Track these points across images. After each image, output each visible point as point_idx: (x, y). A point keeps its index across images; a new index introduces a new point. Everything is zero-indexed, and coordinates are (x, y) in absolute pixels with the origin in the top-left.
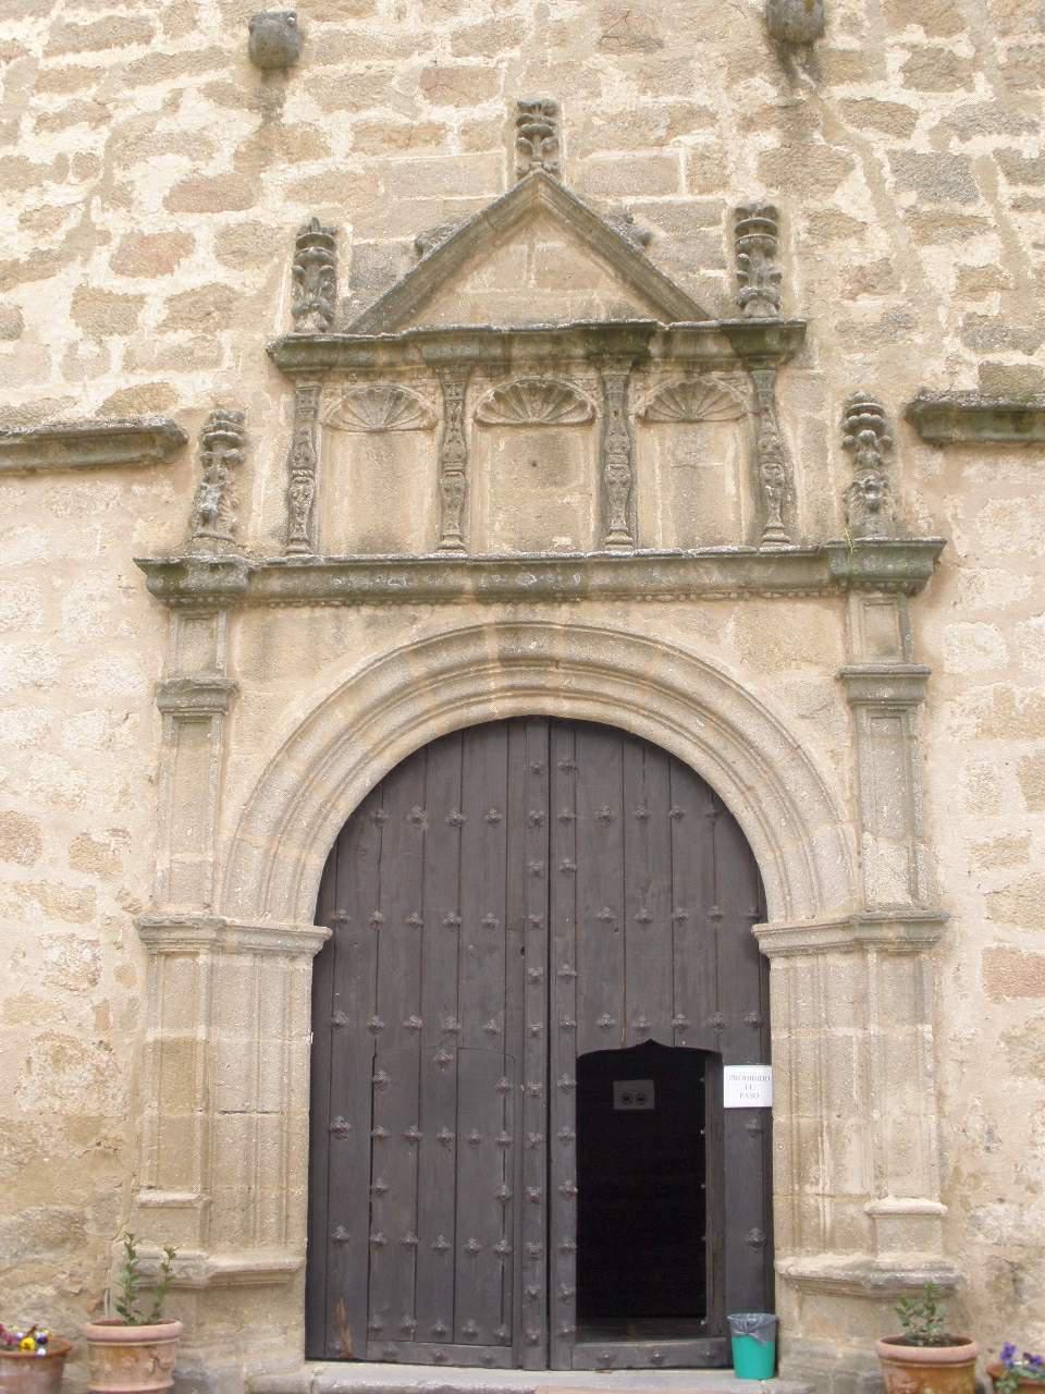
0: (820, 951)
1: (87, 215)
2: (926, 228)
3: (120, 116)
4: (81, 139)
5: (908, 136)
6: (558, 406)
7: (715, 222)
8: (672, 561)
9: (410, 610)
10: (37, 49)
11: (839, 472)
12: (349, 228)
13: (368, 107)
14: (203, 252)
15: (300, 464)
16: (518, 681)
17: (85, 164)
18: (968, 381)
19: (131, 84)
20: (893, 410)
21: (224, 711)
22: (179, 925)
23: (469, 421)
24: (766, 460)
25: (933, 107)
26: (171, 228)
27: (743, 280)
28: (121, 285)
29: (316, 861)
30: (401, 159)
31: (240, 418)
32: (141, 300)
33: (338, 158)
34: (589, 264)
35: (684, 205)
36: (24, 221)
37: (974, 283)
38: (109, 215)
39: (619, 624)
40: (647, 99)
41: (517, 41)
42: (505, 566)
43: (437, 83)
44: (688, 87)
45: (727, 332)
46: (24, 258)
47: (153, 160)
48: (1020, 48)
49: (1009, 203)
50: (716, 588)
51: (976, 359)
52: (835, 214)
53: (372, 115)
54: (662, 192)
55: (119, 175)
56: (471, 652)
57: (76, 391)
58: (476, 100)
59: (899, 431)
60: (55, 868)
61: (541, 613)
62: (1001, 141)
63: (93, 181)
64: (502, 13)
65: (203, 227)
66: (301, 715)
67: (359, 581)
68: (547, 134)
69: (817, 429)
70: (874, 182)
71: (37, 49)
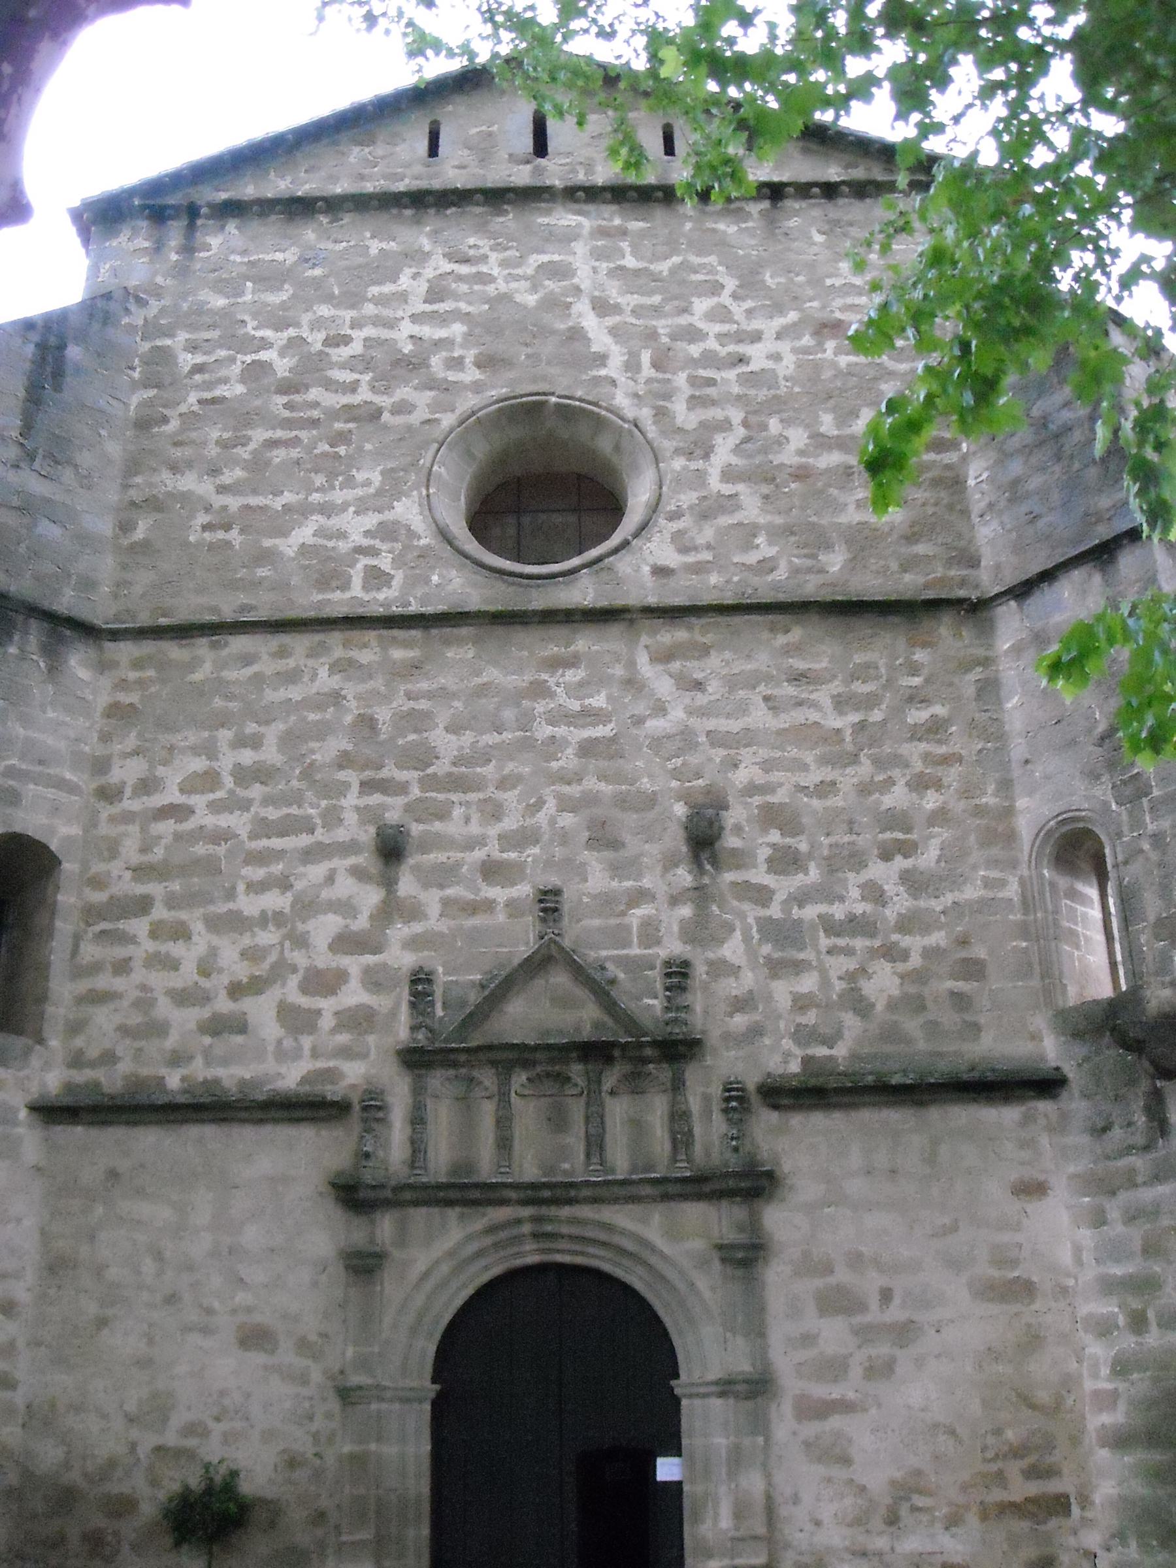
0: (705, 1396)
1: (282, 952)
2: (776, 968)
3: (299, 885)
4: (275, 901)
5: (768, 907)
6: (563, 1084)
7: (652, 968)
8: (624, 1183)
9: (481, 1209)
10: (244, 834)
11: (719, 1125)
12: (440, 970)
13: (449, 886)
14: (354, 983)
15: (417, 1119)
16: (542, 1246)
17: (278, 918)
18: (795, 1067)
20: (751, 1087)
21: (379, 1266)
22: (360, 1388)
23: (513, 1094)
24: (679, 1118)
25: (784, 886)
26: (334, 965)
27: (667, 1009)
28: (304, 1001)
29: (432, 1349)
31: (382, 1092)
32: (319, 1012)
33: (432, 922)
34: (581, 993)
35: (636, 956)
36: (244, 954)
37: (801, 1003)
38: (295, 954)
39: (597, 1217)
40: (615, 884)
41: (537, 841)
42: (533, 1186)
43: (492, 871)
44: (639, 876)
45: (655, 1044)
46: (245, 980)
47: (321, 918)
48: (837, 845)
49: (824, 950)
50: (647, 1196)
51: (799, 1052)
52: (724, 962)
53: (450, 892)
54: (624, 948)
55: (300, 927)
56: (515, 1231)
57: (283, 1070)
58: (513, 884)
59: (755, 1099)
60: (287, 1355)
61: (553, 1211)
62: (822, 908)
63: (284, 931)
64: (529, 822)
65: (354, 964)
66: (423, 1269)
67: (453, 1194)
68: (556, 910)
69: (707, 1098)
70: (747, 939)
71: (244, 834)
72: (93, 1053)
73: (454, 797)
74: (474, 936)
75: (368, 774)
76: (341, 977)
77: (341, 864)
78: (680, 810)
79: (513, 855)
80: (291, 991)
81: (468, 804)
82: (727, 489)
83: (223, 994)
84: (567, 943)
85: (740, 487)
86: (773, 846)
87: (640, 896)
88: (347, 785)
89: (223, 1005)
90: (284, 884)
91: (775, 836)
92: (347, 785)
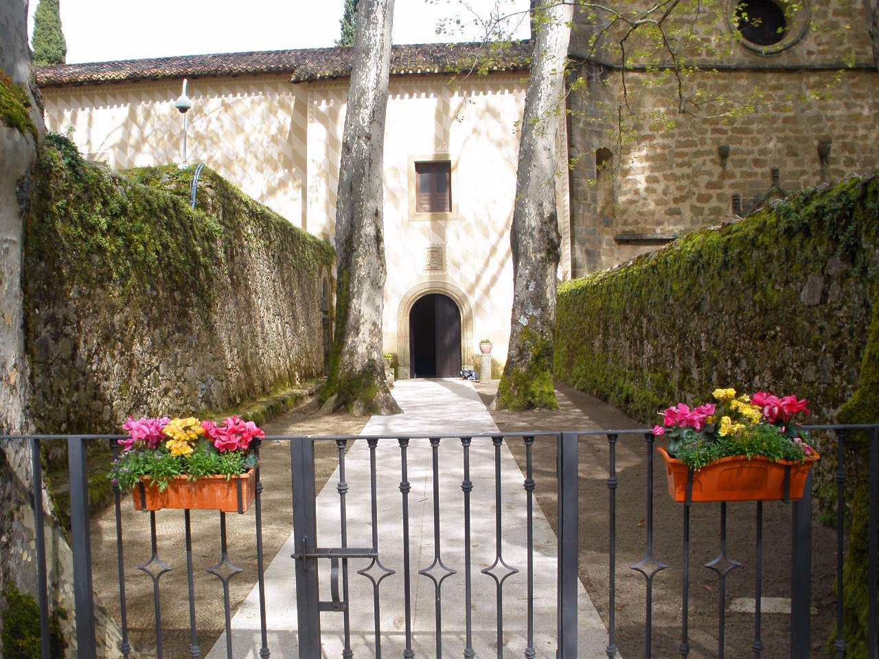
3: (694, 165)
14: (714, 199)
17: (688, 176)
19: (695, 157)
28: (698, 205)
30: (749, 180)
32: (703, 208)
36: (677, 188)
40: (795, 168)
43: (757, 162)
53: (744, 169)
58: (764, 167)
65: (714, 192)
72: (630, 221)
73: (743, 136)
74: (751, 184)
75: (713, 127)
76: (710, 197)
77: (708, 158)
78: (816, 143)
79: (763, 157)
80: (693, 200)
81: (747, 139)
82: (835, 19)
83: (672, 202)
84: (781, 187)
85: (839, 18)
86: (846, 157)
87: (803, 173)
88: (707, 130)
89: (672, 205)
90: (690, 166)
91: (847, 154)
92: (707, 130)
